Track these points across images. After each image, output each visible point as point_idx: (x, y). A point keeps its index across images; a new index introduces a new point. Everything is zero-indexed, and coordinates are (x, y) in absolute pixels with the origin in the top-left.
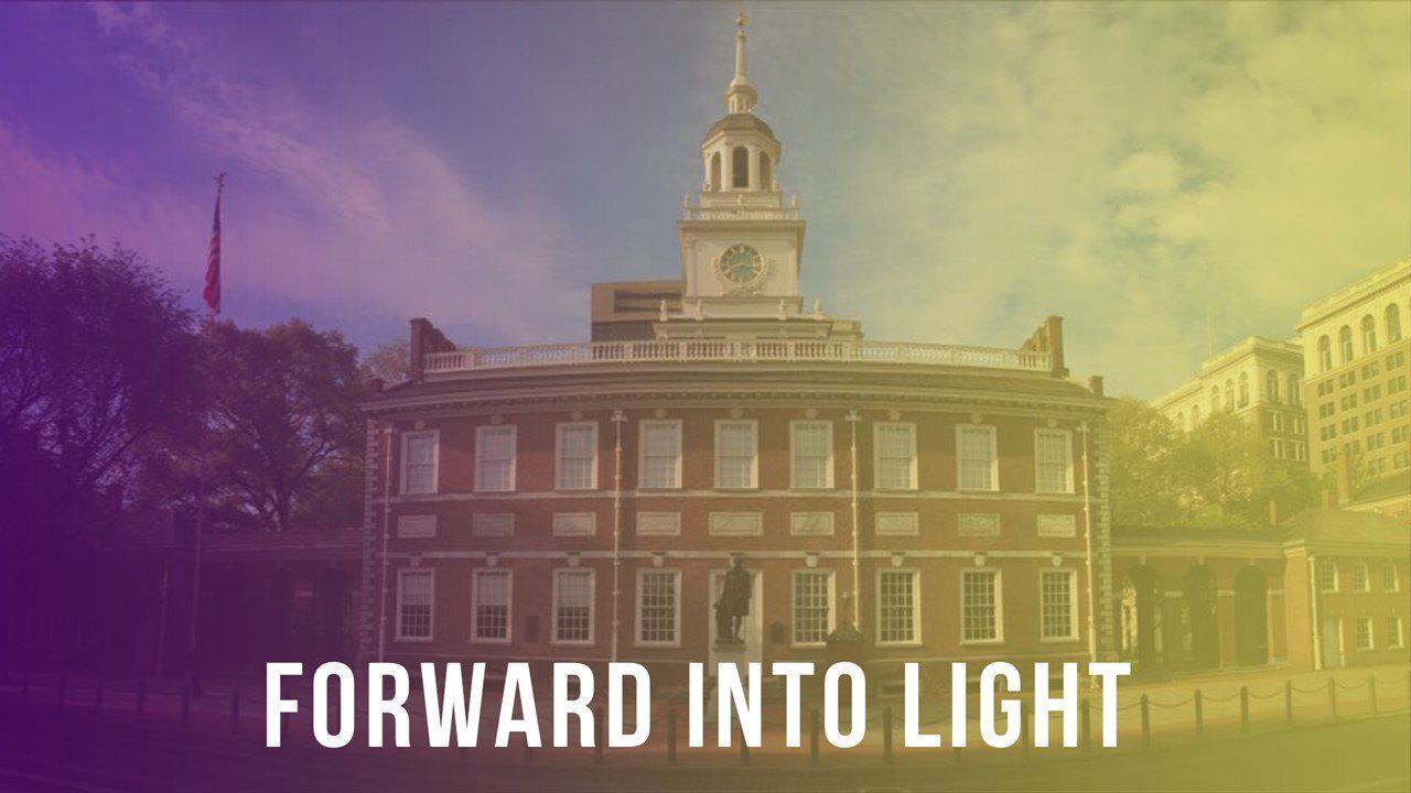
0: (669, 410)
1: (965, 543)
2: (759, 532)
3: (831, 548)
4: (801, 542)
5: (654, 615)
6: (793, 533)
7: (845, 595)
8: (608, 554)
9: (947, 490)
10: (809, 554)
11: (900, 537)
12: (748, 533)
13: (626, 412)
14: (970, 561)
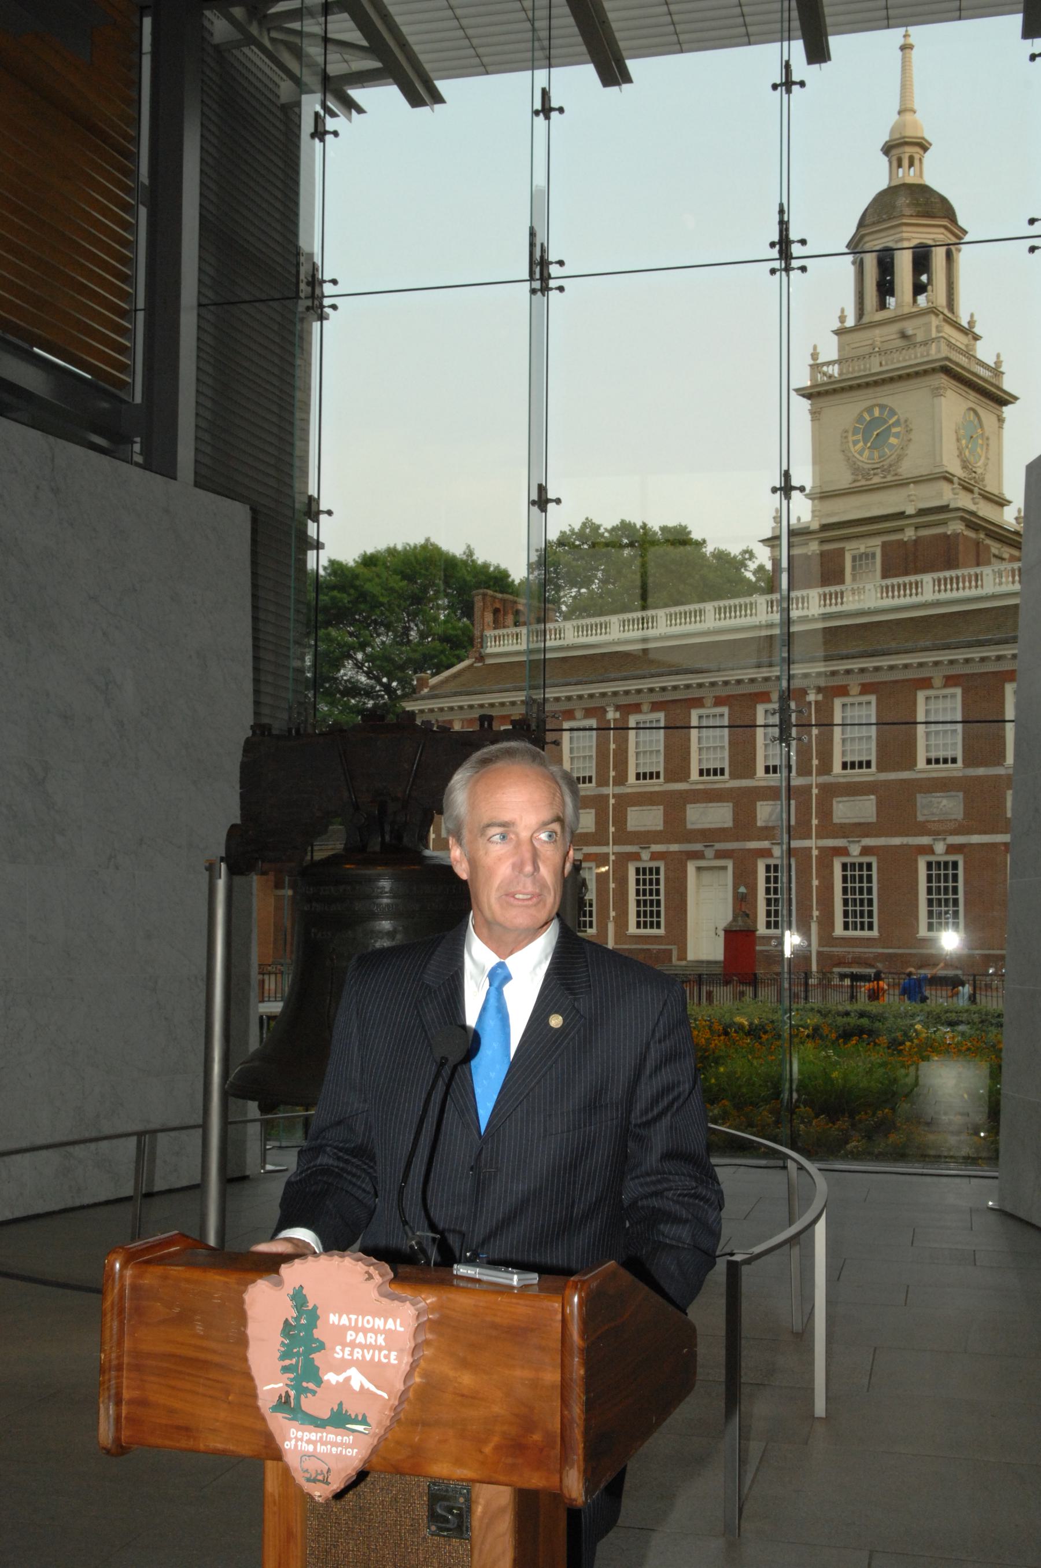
0: (653, 703)
1: (923, 829)
2: (729, 823)
4: (767, 832)
5: (645, 906)
6: (759, 824)
7: (742, 890)
8: (618, 849)
9: (906, 770)
10: (773, 844)
11: (860, 824)
12: (719, 826)
13: (618, 708)
14: (929, 850)
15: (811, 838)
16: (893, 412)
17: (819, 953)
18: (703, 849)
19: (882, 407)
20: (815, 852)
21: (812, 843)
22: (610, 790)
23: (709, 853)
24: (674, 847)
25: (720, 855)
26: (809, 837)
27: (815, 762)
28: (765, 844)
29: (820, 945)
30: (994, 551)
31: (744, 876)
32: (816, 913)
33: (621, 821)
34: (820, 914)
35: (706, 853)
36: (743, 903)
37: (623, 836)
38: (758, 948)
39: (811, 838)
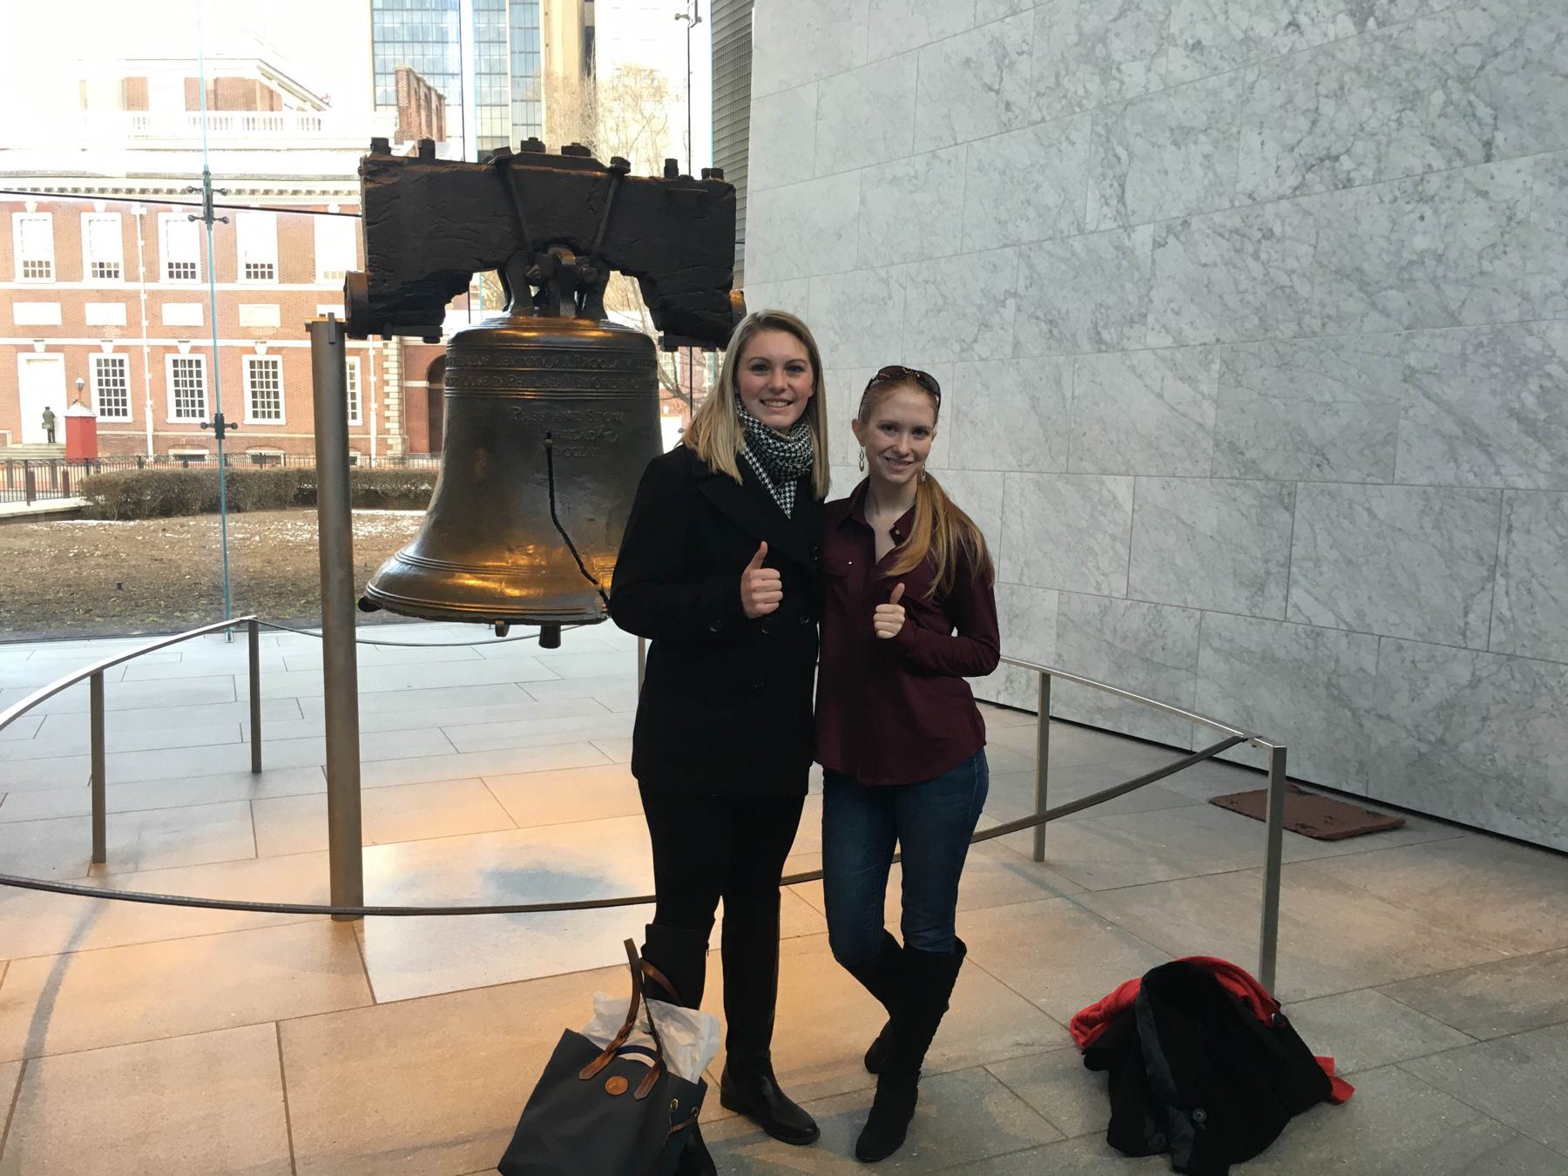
3: (123, 336)
4: (98, 330)
7: (80, 381)
14: (253, 351)
15: (142, 337)
17: (154, 436)
18: (33, 343)
20: (146, 350)
21: (145, 342)
23: (39, 347)
25: (49, 349)
26: (139, 336)
27: (142, 270)
28: (96, 342)
29: (155, 430)
30: (284, 101)
31: (74, 368)
32: (149, 402)
34: (155, 403)
35: (36, 347)
36: (77, 393)
38: (98, 432)
39: (142, 337)
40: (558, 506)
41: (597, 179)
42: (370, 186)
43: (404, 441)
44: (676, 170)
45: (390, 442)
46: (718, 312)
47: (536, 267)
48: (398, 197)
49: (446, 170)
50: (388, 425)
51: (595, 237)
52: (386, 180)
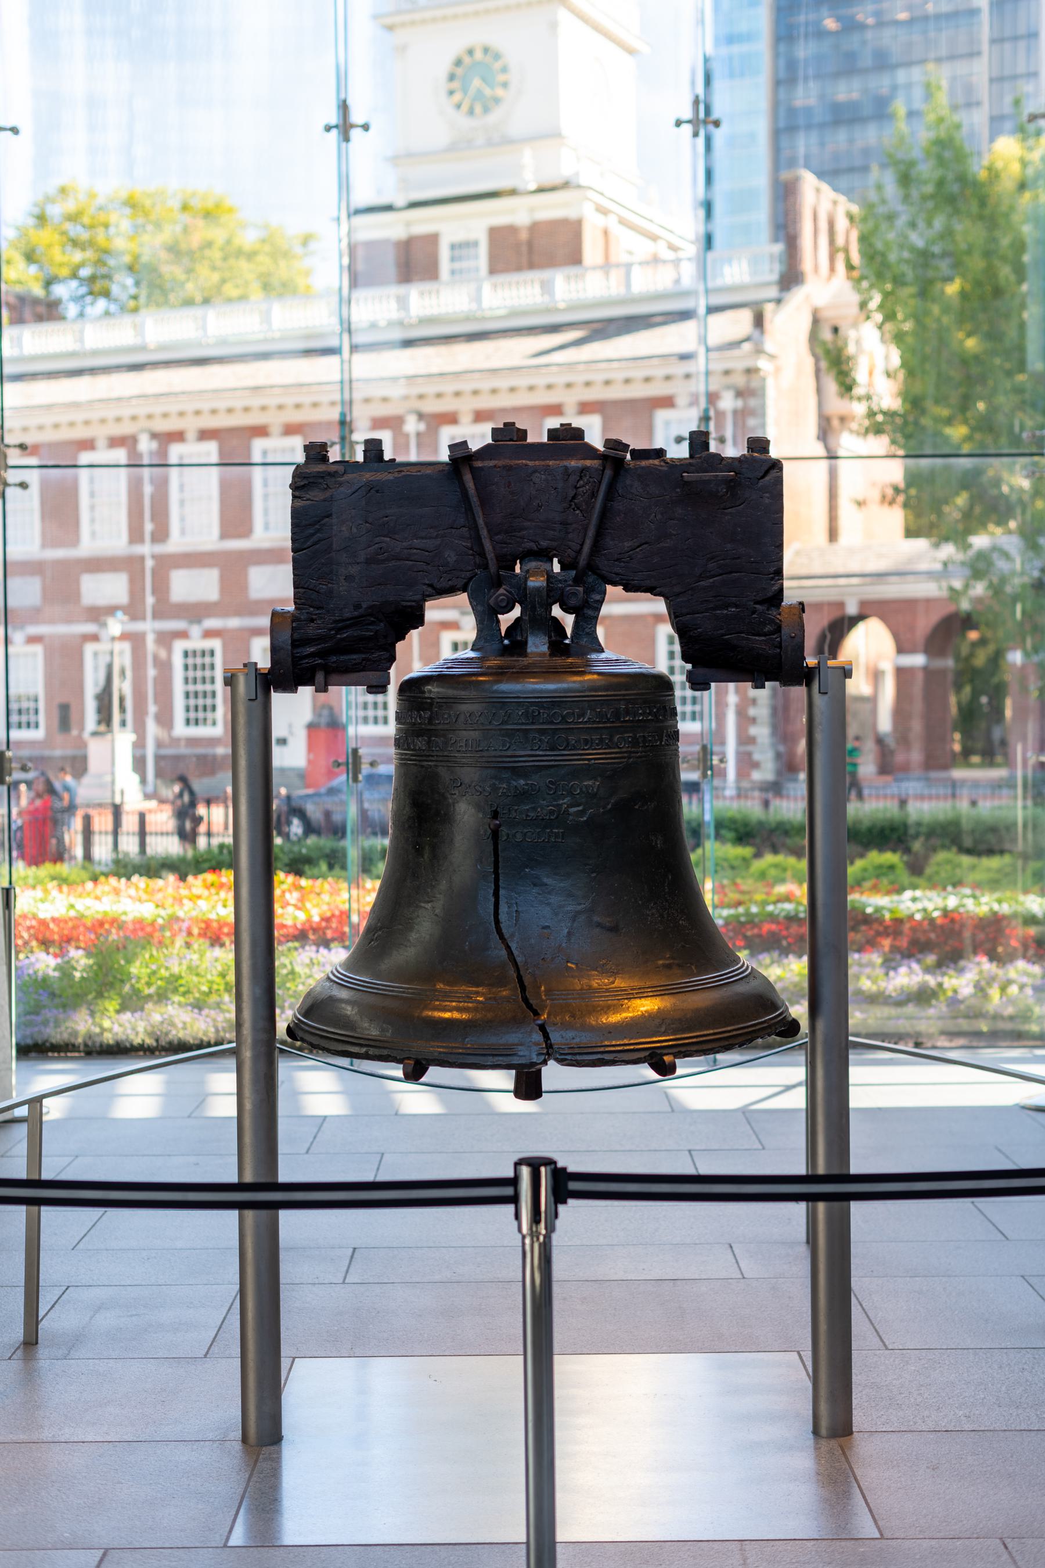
13: (154, 436)
16: (497, 56)
19: (486, 50)
22: (146, 549)
24: (234, 623)
33: (161, 587)
37: (164, 609)
40: (503, 908)
41: (583, 470)
42: (300, 503)
43: (778, 756)
44: (706, 446)
45: (757, 757)
46: (759, 635)
47: (502, 591)
48: (329, 516)
49: (390, 477)
50: (753, 731)
51: (582, 545)
52: (316, 495)
